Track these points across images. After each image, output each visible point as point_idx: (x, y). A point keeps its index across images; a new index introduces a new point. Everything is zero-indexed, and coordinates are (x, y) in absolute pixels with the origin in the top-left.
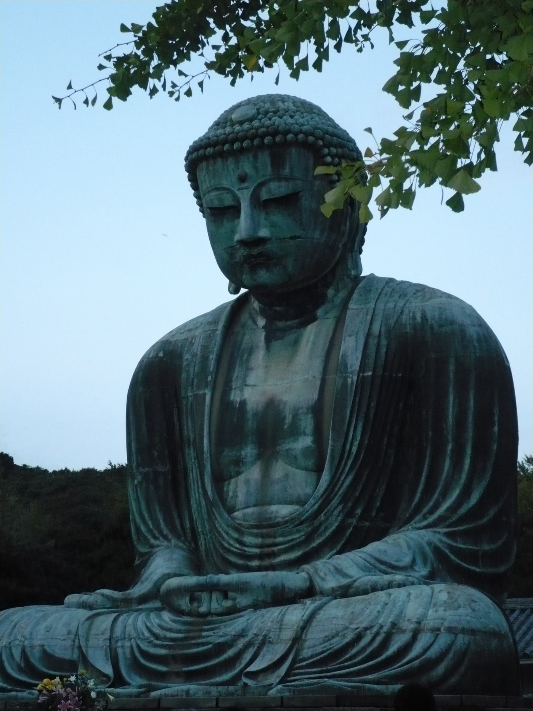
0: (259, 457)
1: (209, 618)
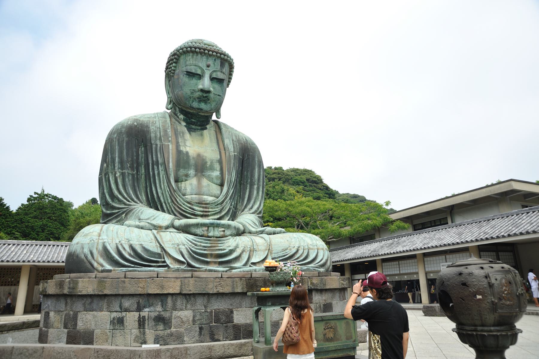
0: (196, 175)
1: (212, 239)
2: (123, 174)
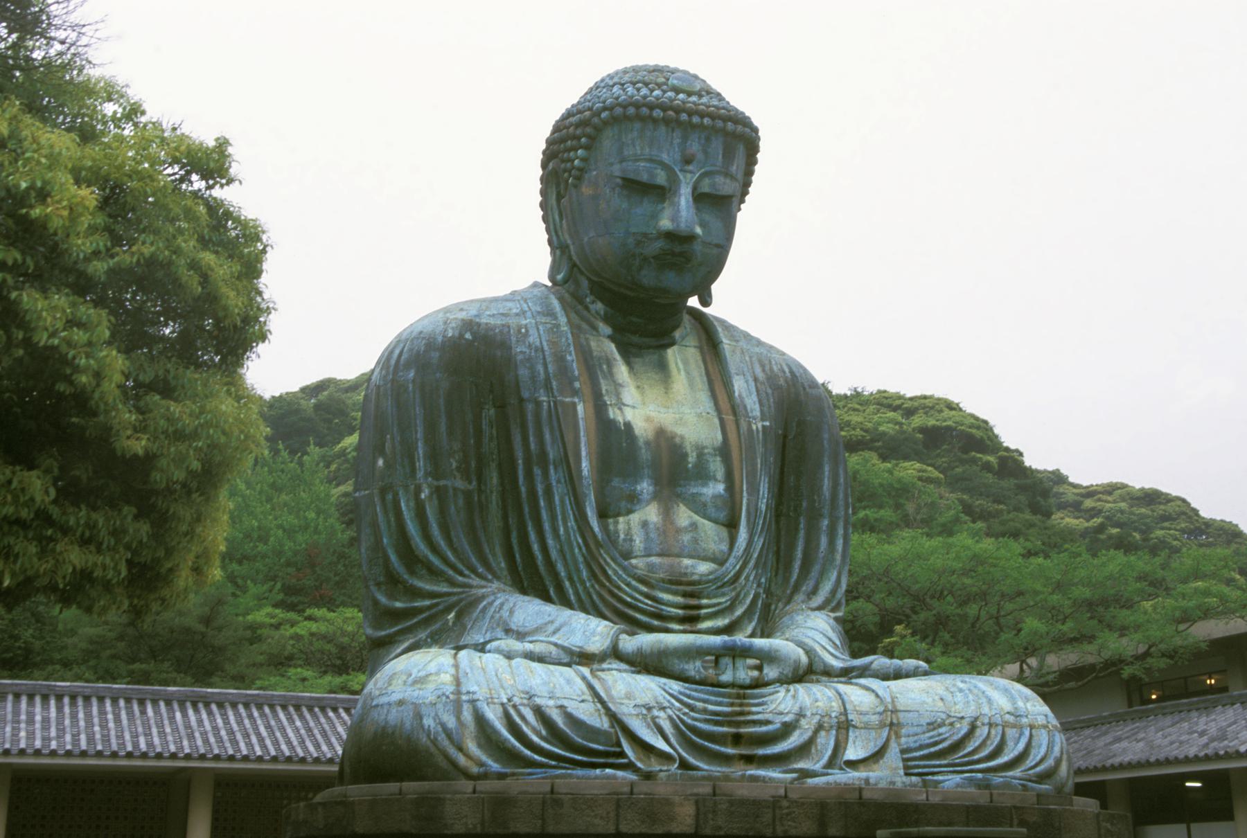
2: (439, 493)
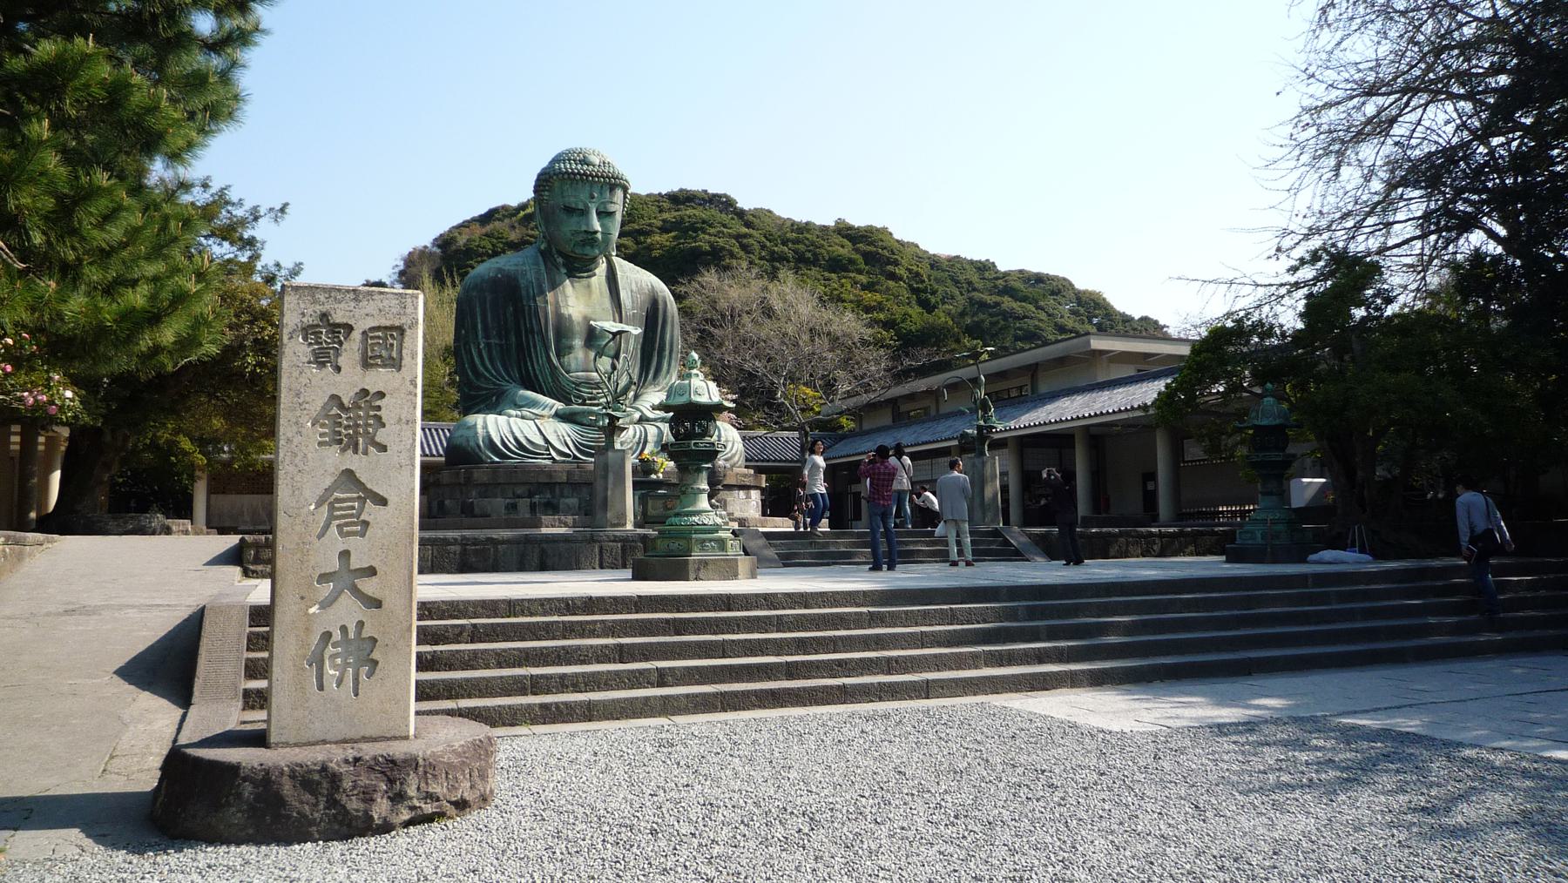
2: (488, 345)
